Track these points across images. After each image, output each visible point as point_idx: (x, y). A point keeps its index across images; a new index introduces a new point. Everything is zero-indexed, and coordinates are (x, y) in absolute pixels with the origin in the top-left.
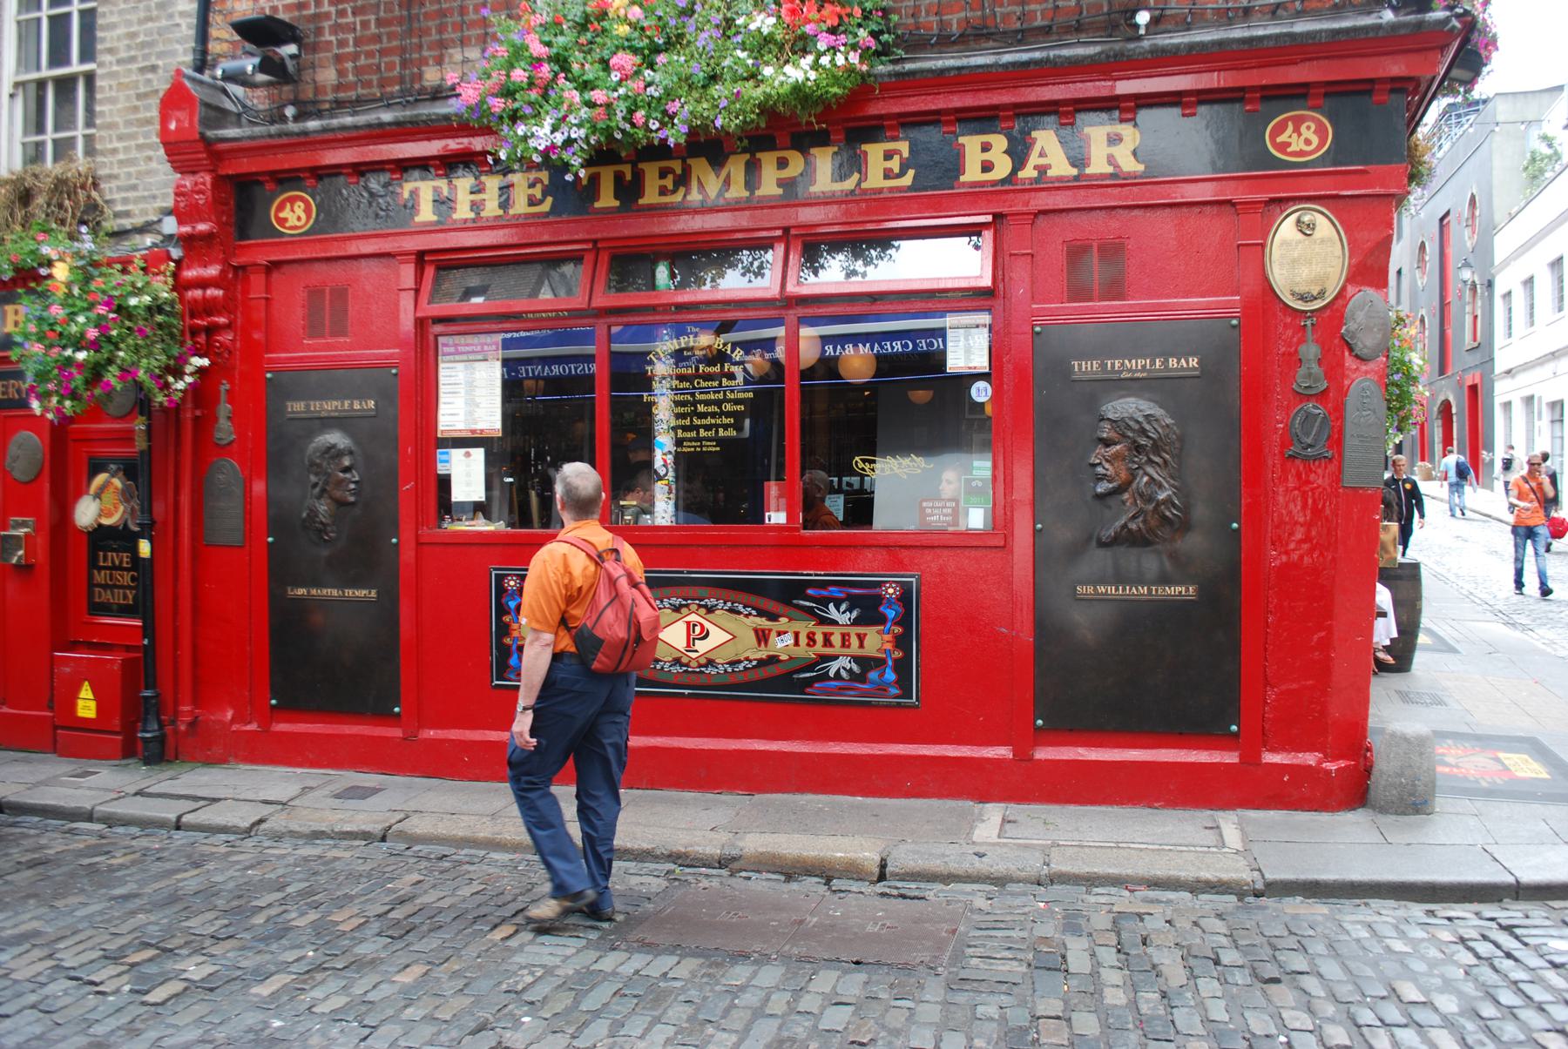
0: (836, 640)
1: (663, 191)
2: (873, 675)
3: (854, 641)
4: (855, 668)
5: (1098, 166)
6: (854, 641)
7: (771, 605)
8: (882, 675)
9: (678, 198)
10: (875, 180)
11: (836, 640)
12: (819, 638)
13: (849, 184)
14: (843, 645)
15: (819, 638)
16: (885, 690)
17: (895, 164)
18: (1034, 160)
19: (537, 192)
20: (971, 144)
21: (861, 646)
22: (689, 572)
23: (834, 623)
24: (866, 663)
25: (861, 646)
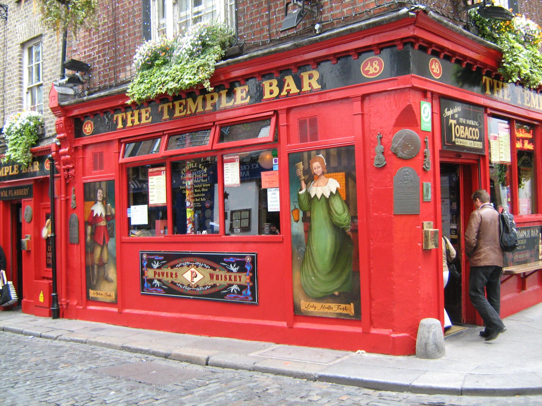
0: (233, 278)
2: (244, 292)
3: (238, 279)
4: (239, 289)
6: (238, 279)
7: (214, 265)
8: (246, 292)
11: (233, 278)
12: (228, 277)
14: (235, 280)
15: (228, 277)
16: (247, 298)
21: (240, 280)
22: (191, 252)
23: (232, 271)
24: (242, 287)
25: (240, 280)
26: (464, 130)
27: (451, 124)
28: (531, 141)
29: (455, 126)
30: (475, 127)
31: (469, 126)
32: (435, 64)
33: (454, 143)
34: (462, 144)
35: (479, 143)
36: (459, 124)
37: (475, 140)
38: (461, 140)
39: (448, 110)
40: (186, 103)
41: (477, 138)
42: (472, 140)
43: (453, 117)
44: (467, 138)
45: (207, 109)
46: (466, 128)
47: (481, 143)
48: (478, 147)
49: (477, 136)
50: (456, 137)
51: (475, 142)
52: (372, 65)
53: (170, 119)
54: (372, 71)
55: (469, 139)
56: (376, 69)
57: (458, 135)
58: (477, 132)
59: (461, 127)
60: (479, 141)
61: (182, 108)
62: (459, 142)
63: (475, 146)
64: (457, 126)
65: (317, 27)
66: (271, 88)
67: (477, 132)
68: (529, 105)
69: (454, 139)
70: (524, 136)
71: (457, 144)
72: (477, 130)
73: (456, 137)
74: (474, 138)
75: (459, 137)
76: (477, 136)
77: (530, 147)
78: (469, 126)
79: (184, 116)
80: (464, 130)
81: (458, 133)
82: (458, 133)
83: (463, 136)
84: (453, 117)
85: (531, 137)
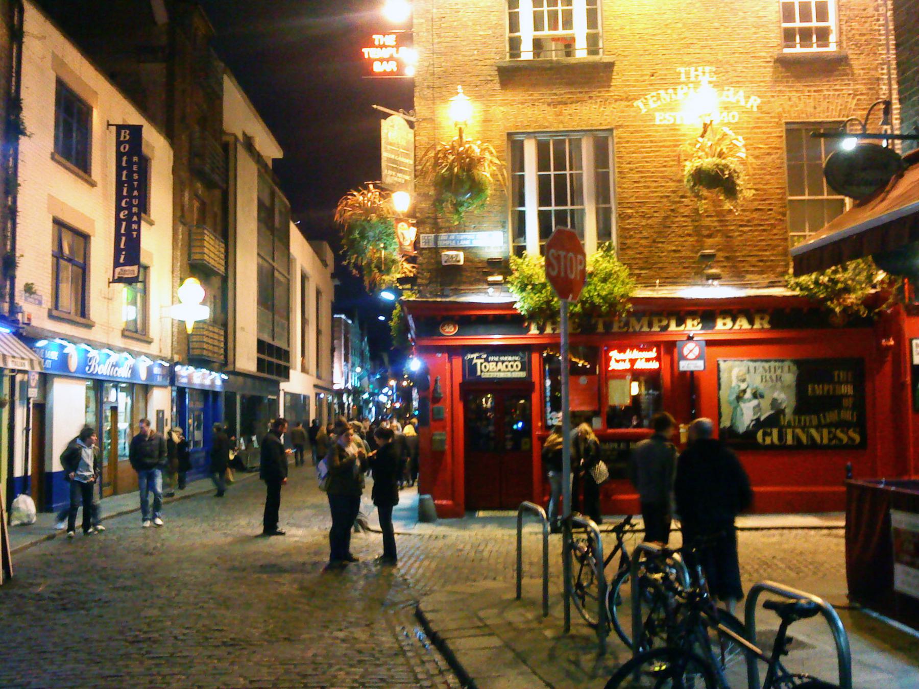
1: (620, 327)
9: (625, 329)
13: (682, 328)
26: (496, 365)
27: (476, 364)
29: (481, 364)
30: (515, 361)
31: (503, 362)
33: (480, 376)
36: (489, 362)
37: (514, 371)
42: (509, 371)
43: (477, 358)
44: (500, 371)
55: (504, 372)
59: (491, 364)
60: (521, 370)
62: (485, 375)
68: (625, 329)
69: (479, 373)
72: (516, 363)
73: (482, 371)
74: (512, 370)
75: (488, 371)
77: (655, 365)
78: (503, 362)
80: (496, 365)
81: (485, 367)
82: (485, 367)
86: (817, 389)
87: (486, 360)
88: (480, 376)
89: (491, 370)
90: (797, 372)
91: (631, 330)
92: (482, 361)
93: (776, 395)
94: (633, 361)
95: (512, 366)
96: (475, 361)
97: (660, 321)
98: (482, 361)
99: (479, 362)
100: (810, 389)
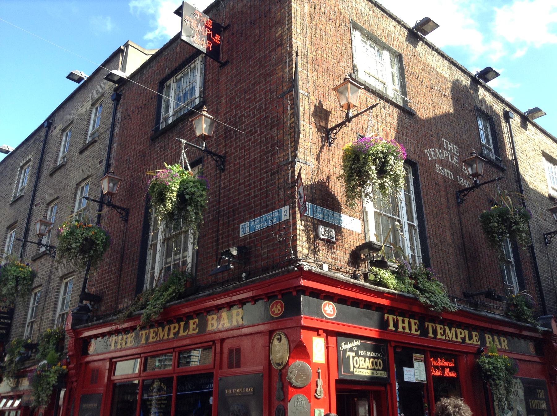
1: (442, 335)
5: (503, 347)
10: (475, 343)
17: (477, 338)
18: (495, 343)
19: (416, 327)
20: (487, 336)
26: (365, 362)
27: (349, 357)
28: (451, 369)
29: (353, 357)
30: (378, 358)
32: (328, 306)
33: (353, 372)
34: (362, 374)
35: (383, 372)
37: (378, 370)
38: (360, 370)
39: (346, 344)
40: (158, 330)
41: (381, 368)
43: (351, 350)
45: (170, 337)
46: (367, 359)
47: (386, 372)
48: (382, 376)
49: (380, 366)
50: (354, 367)
51: (378, 372)
52: (276, 307)
53: (146, 343)
54: (277, 312)
56: (279, 310)
57: (357, 366)
58: (380, 363)
59: (361, 358)
60: (382, 370)
61: (154, 335)
63: (378, 375)
64: (356, 358)
65: (244, 275)
66: (213, 322)
67: (380, 363)
68: (444, 337)
69: (352, 370)
70: (443, 365)
71: (355, 373)
72: (380, 360)
73: (354, 367)
74: (377, 368)
75: (359, 368)
76: (380, 366)
77: (453, 374)
79: (155, 342)
80: (365, 362)
81: (357, 363)
82: (357, 363)
83: (363, 367)
84: (351, 350)
85: (453, 365)
86: (534, 404)
87: (357, 355)
88: (353, 372)
89: (361, 366)
90: (523, 388)
91: (447, 338)
92: (354, 354)
93: (518, 409)
94: (443, 368)
95: (376, 363)
96: (348, 354)
97: (461, 334)
98: (354, 354)
99: (351, 354)
100: (530, 404)
